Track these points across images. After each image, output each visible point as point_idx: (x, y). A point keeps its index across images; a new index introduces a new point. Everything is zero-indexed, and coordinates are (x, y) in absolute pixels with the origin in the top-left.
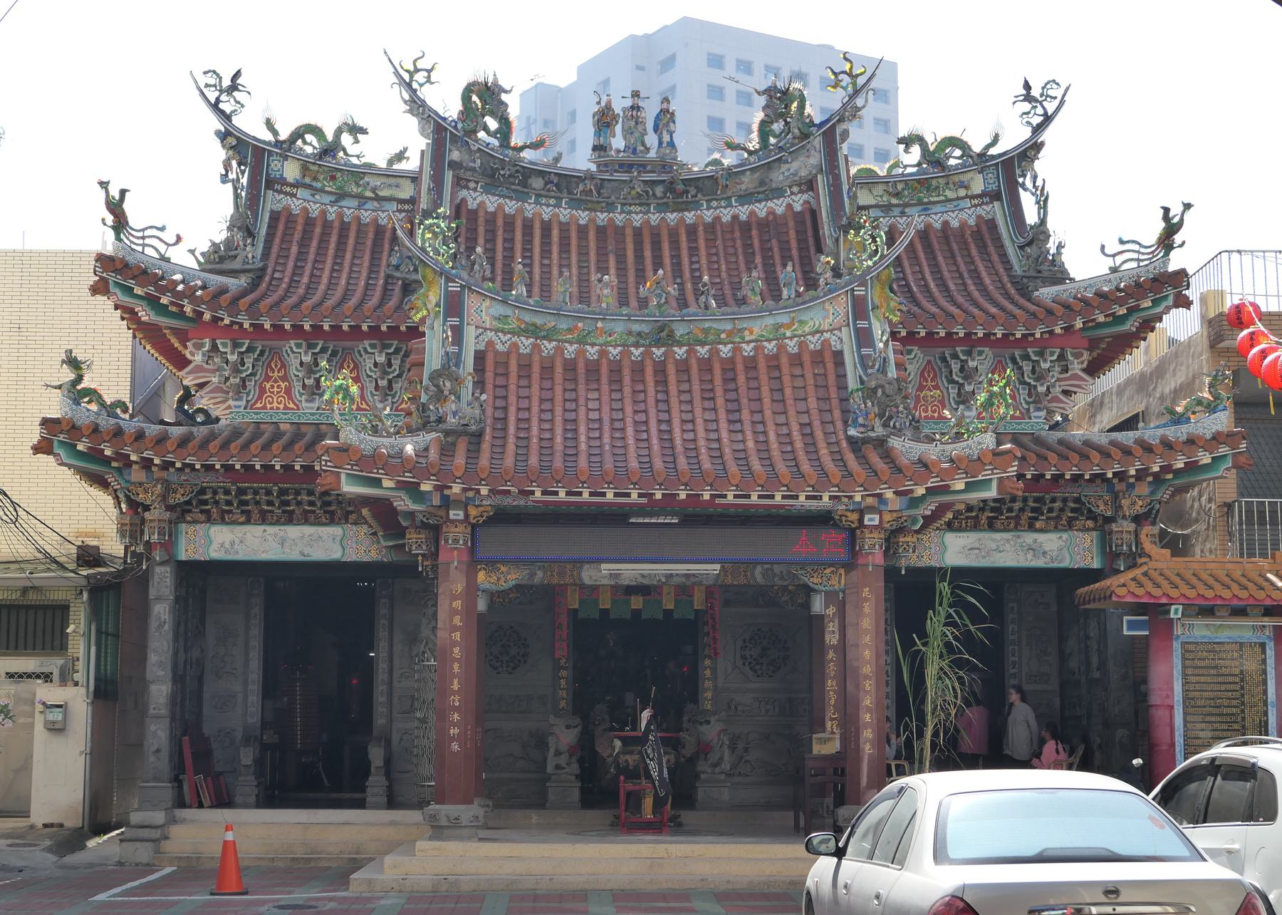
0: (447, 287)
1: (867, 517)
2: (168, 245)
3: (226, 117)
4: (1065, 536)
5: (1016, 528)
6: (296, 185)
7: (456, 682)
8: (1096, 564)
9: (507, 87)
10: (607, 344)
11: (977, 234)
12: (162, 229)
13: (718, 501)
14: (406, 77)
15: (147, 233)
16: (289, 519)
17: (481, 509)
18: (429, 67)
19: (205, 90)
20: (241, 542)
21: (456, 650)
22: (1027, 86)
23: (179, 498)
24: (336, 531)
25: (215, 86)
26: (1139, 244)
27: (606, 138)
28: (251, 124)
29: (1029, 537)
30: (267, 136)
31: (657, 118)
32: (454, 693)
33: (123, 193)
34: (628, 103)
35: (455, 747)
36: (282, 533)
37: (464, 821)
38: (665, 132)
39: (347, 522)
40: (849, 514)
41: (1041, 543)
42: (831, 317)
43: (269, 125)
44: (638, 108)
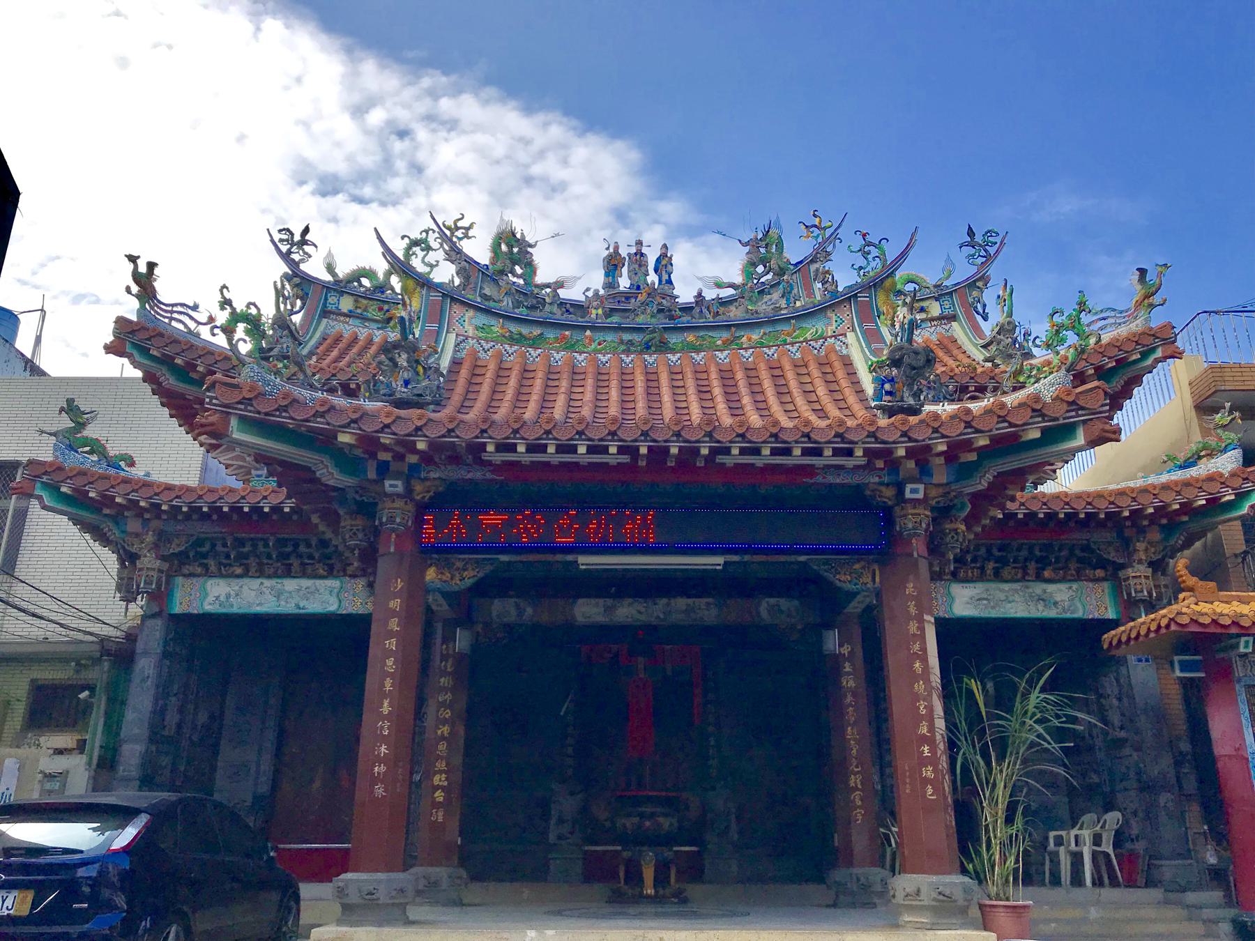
0: (428, 296)
1: (909, 487)
2: (199, 323)
3: (294, 265)
4: (1075, 586)
5: (1023, 579)
6: (350, 315)
7: (386, 703)
8: (1111, 614)
9: (532, 241)
10: (596, 352)
11: (941, 344)
12: (195, 308)
13: (720, 459)
14: (448, 233)
15: (175, 309)
16: (288, 573)
17: (428, 483)
18: (467, 226)
19: (279, 244)
20: (237, 595)
21: (390, 662)
22: (971, 233)
23: (175, 548)
24: (334, 583)
25: (287, 240)
26: (1114, 310)
27: (613, 277)
28: (315, 268)
29: (1038, 588)
30: (327, 277)
31: (658, 261)
32: (383, 718)
33: (151, 266)
34: (633, 250)
35: (379, 790)
36: (279, 586)
37: (383, 897)
38: (664, 273)
39: (345, 575)
40: (883, 489)
41: (1051, 593)
42: (835, 325)
43: (330, 269)
44: (642, 255)
